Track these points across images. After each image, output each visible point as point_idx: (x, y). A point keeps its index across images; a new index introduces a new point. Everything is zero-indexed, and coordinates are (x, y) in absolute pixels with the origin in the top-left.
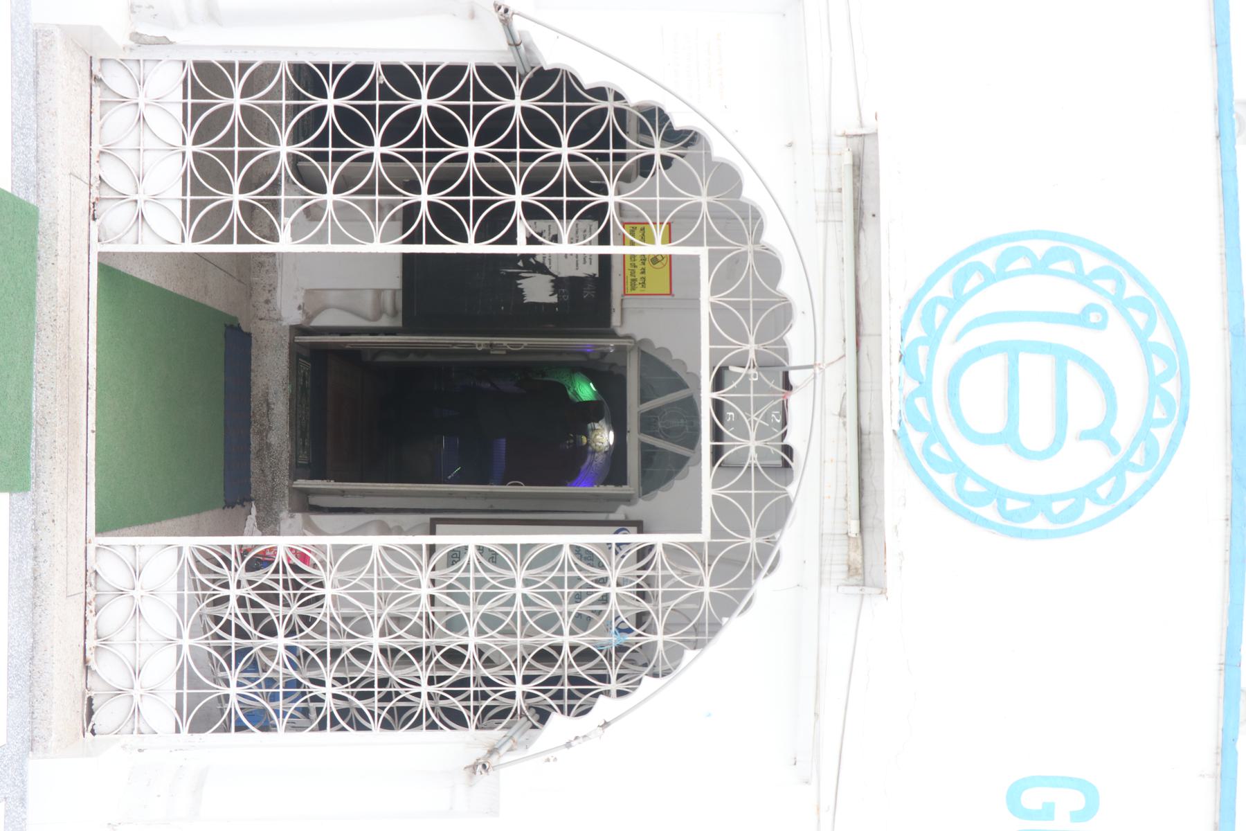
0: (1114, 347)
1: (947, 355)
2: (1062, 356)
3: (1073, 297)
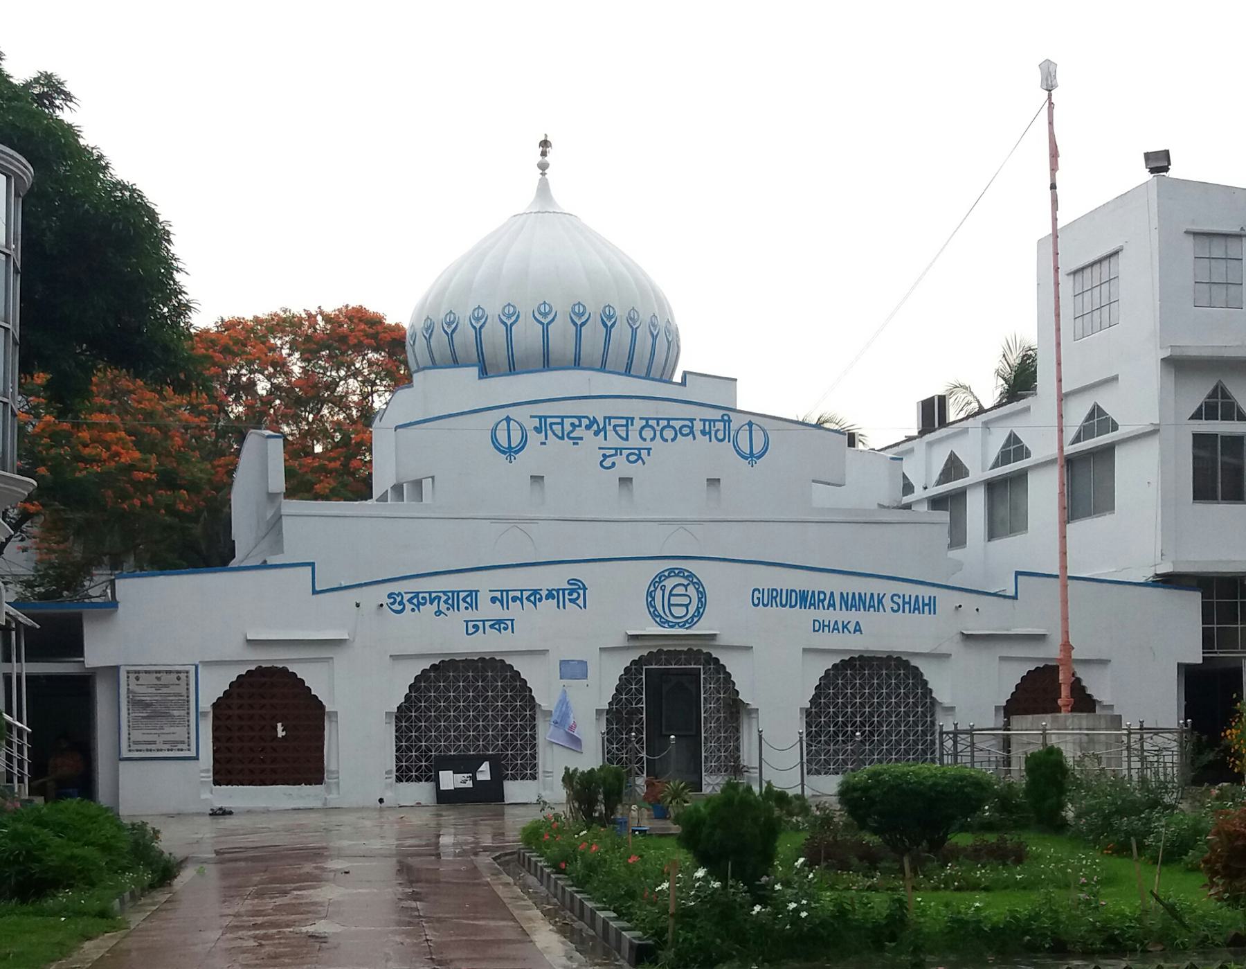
0: (669, 583)
1: (671, 619)
2: (671, 594)
3: (659, 593)
